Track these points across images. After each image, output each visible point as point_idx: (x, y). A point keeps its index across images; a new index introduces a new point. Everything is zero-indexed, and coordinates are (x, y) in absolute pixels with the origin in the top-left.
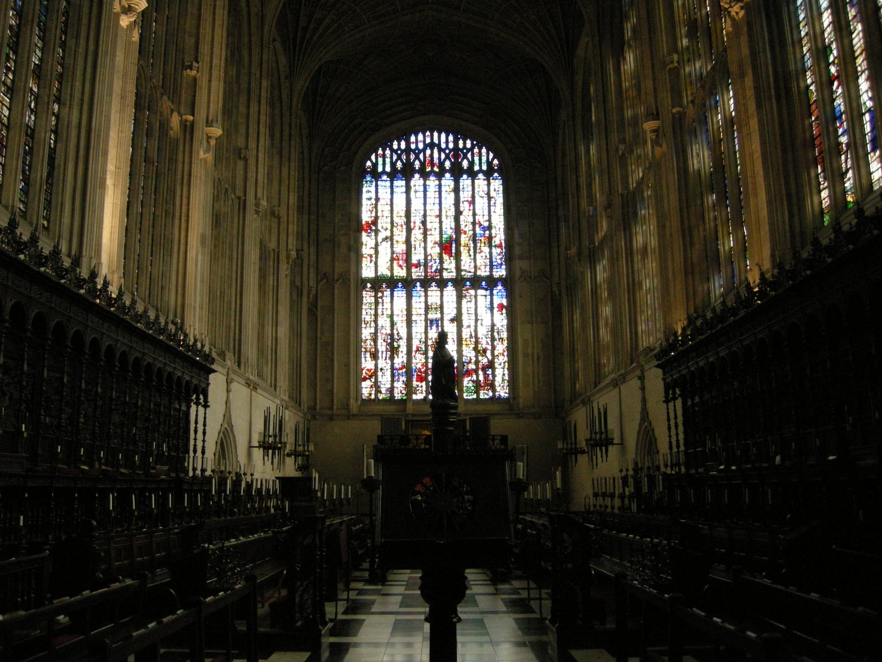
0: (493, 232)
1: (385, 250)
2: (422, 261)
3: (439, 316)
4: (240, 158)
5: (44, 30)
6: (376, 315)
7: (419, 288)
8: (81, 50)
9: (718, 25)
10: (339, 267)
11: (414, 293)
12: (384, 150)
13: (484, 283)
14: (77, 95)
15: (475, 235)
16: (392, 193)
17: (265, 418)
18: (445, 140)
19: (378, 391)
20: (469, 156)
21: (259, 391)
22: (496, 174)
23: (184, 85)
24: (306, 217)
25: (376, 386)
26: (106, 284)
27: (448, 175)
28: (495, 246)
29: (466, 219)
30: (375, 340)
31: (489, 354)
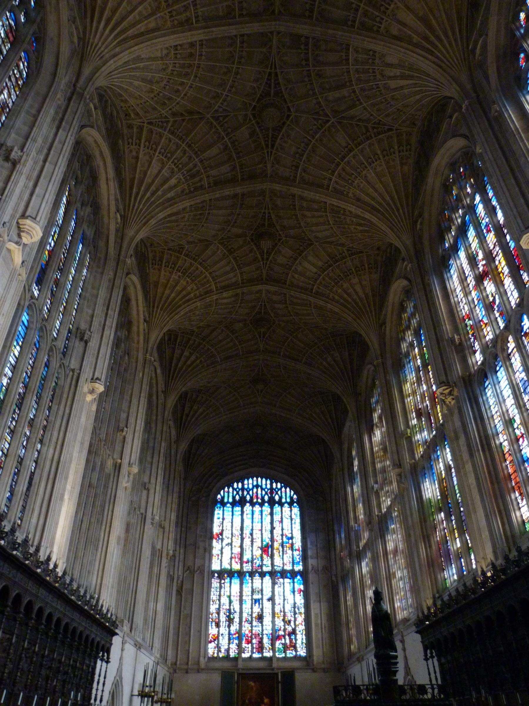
0: (294, 540)
1: (227, 551)
2: (250, 559)
3: (259, 596)
4: (145, 488)
5: (39, 398)
6: (220, 596)
7: (248, 577)
8: (61, 413)
9: (435, 411)
10: (198, 562)
11: (245, 581)
12: (228, 488)
13: (289, 575)
14: (54, 439)
15: (283, 542)
16: (233, 515)
17: (145, 671)
18: (265, 483)
19: (219, 651)
20: (279, 492)
21: (142, 650)
22: (295, 504)
23: (117, 441)
24: (179, 529)
25: (218, 647)
26: (56, 566)
27: (266, 504)
28: (296, 550)
29: (277, 532)
30: (218, 613)
31: (292, 623)
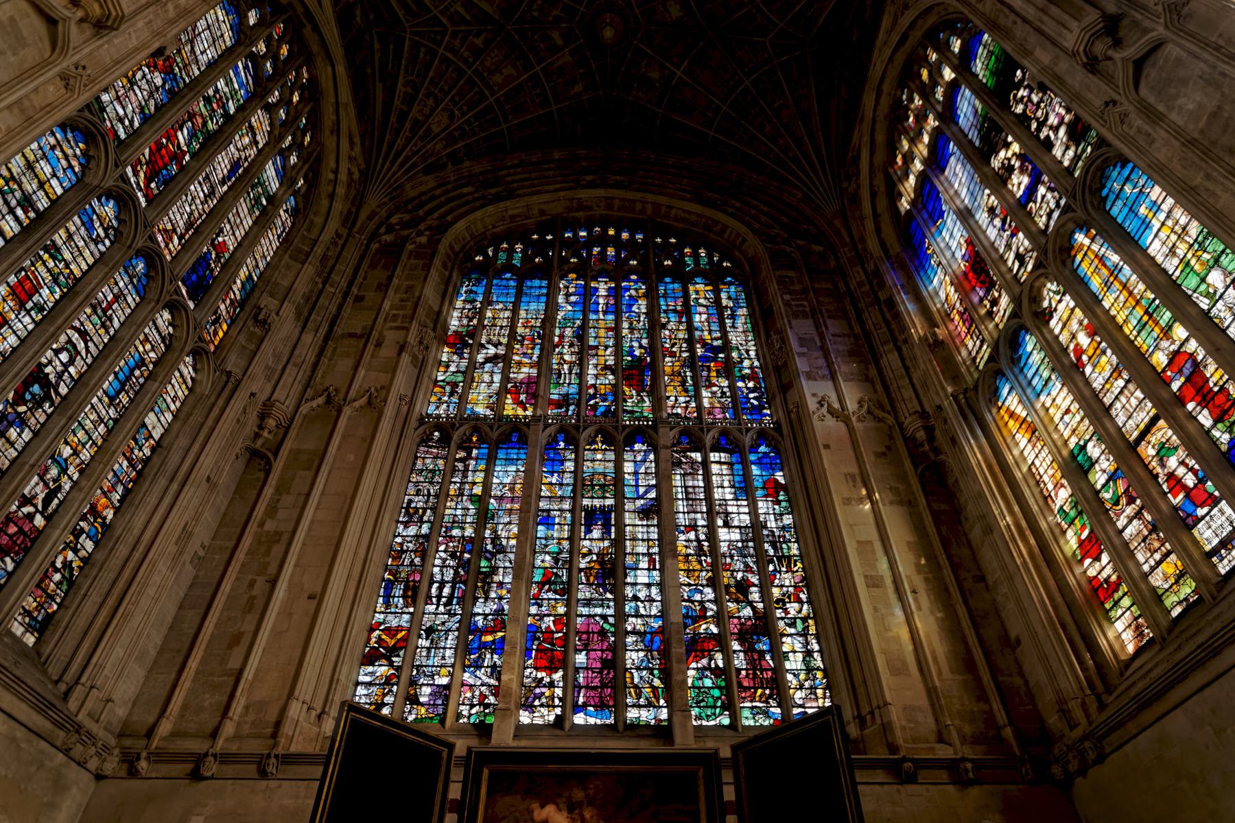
31: (755, 595)
